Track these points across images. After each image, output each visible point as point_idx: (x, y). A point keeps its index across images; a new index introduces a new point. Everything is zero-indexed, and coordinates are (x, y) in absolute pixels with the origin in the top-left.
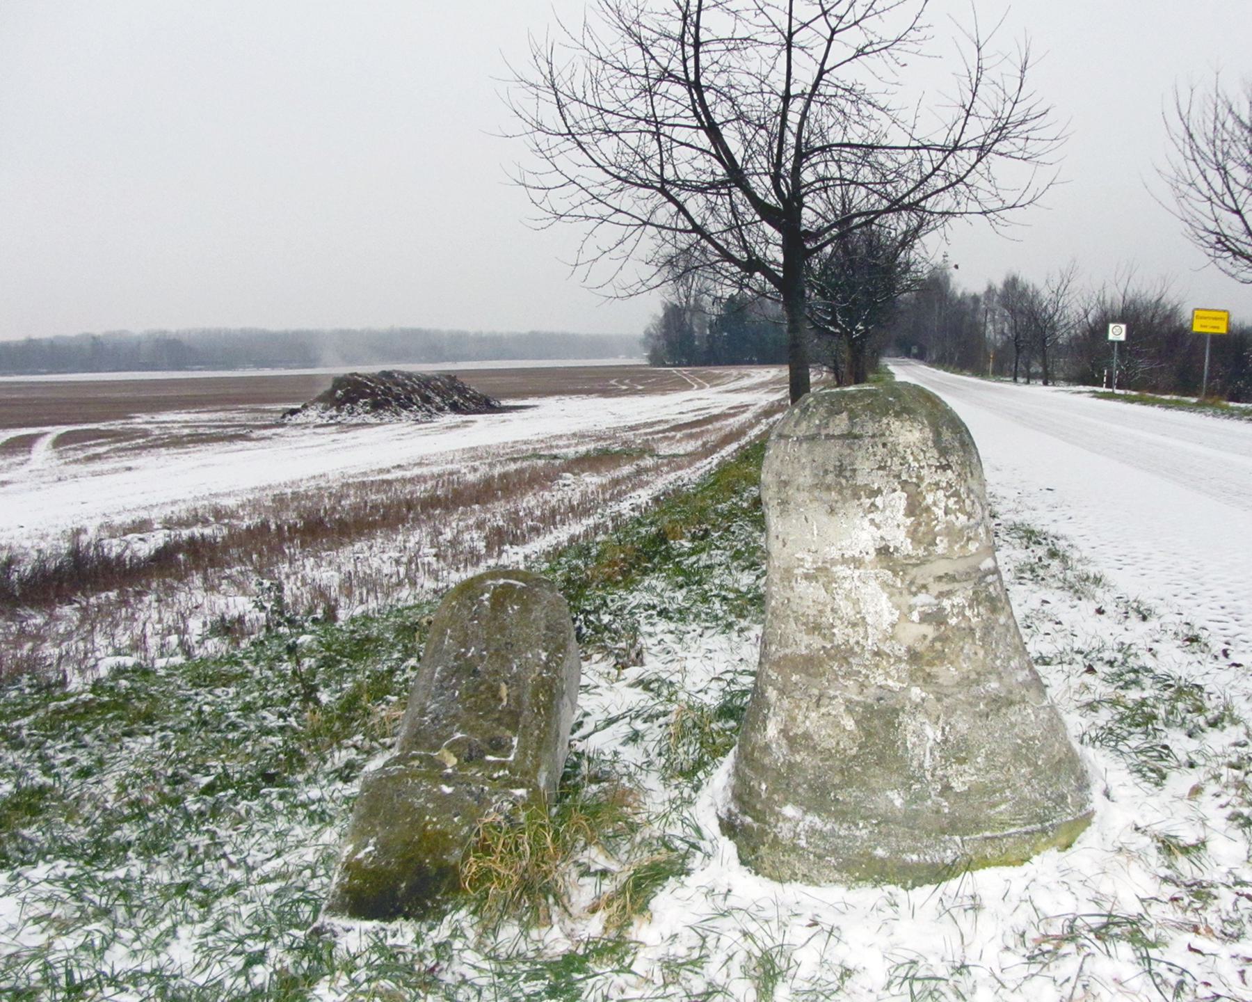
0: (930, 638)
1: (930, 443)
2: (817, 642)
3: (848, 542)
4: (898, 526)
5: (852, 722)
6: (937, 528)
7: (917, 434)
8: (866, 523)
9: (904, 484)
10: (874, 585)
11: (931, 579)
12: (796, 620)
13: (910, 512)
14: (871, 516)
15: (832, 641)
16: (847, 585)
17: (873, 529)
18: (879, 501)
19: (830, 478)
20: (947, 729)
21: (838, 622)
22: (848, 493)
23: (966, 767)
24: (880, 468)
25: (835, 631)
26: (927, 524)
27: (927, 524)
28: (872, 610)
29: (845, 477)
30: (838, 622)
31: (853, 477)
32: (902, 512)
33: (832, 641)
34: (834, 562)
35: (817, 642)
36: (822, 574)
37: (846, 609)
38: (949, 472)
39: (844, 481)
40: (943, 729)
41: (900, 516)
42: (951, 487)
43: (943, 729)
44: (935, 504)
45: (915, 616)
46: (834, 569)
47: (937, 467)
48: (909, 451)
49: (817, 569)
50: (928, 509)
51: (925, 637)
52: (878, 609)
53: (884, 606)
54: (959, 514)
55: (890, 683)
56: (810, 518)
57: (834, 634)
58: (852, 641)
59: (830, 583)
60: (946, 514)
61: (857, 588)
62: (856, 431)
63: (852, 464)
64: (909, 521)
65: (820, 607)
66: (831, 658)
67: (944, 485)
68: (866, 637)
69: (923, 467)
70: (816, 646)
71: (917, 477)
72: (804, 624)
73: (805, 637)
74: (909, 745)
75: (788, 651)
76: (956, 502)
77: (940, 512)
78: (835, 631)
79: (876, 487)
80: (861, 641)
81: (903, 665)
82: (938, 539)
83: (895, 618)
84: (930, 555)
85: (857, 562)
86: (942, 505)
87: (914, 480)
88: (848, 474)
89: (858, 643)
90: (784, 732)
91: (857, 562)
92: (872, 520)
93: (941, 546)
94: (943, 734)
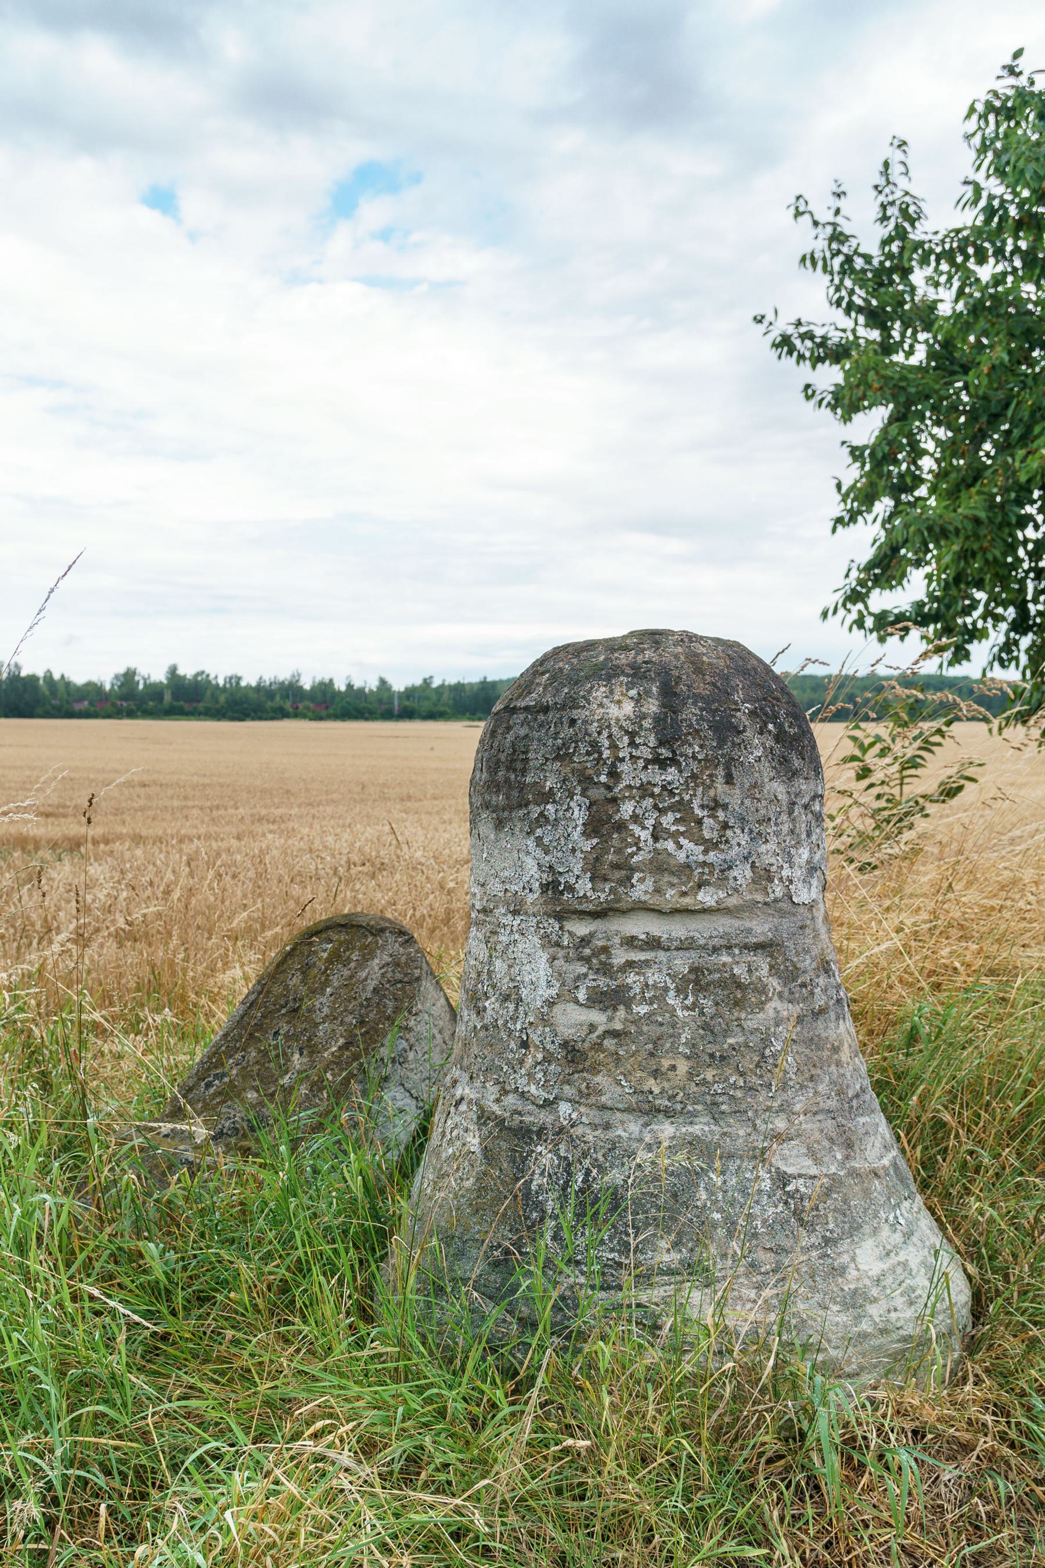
0: (600, 1030)
1: (647, 723)
4: (574, 850)
5: (476, 1141)
6: (635, 859)
7: (628, 708)
11: (617, 940)
13: (594, 827)
14: (539, 832)
17: (539, 853)
24: (558, 758)
26: (619, 851)
27: (619, 851)
29: (515, 770)
31: (524, 771)
40: (588, 1173)
41: (576, 835)
42: (672, 793)
43: (588, 1173)
44: (635, 818)
45: (582, 995)
48: (605, 734)
50: (621, 827)
51: (592, 1027)
54: (683, 841)
55: (533, 1089)
60: (656, 838)
63: (526, 752)
64: (587, 845)
68: (514, 1019)
69: (622, 760)
76: (677, 821)
77: (645, 835)
82: (637, 876)
83: (553, 992)
86: (650, 823)
87: (603, 778)
88: (519, 765)
92: (539, 840)
93: (641, 889)
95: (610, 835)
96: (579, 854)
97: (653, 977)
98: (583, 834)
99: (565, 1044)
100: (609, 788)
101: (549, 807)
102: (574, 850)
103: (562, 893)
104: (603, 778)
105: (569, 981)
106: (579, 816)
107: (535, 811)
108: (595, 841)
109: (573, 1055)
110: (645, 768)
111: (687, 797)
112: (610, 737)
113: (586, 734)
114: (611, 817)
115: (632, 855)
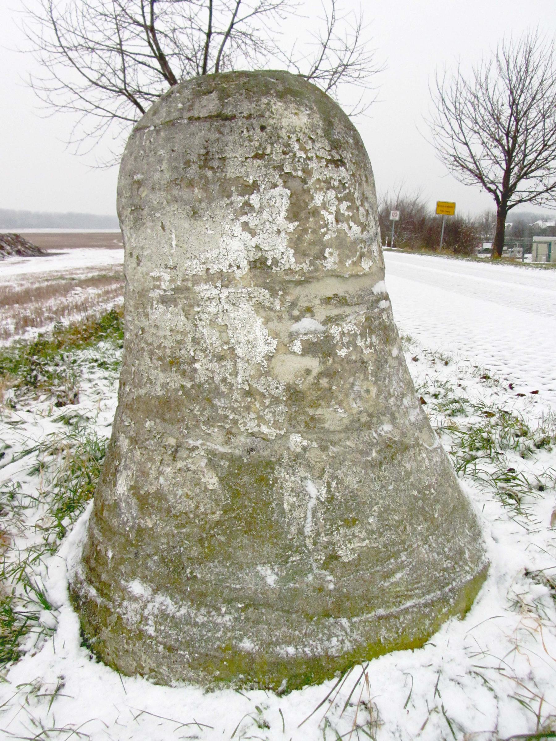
0: (314, 373)
1: (320, 132)
2: (175, 380)
3: (215, 253)
4: (279, 232)
5: (215, 480)
6: (327, 237)
8: (237, 229)
9: (287, 178)
10: (246, 307)
11: (317, 301)
12: (151, 354)
13: (294, 214)
14: (244, 219)
15: (192, 379)
16: (212, 308)
17: (246, 236)
18: (254, 199)
19: (193, 171)
20: (334, 484)
21: (200, 355)
22: (215, 188)
23: (356, 530)
24: (257, 156)
25: (197, 366)
26: (315, 232)
27: (315, 232)
28: (243, 339)
29: (212, 168)
30: (200, 355)
32: (283, 214)
33: (192, 379)
34: (196, 280)
35: (175, 380)
36: (181, 294)
37: (210, 336)
38: (342, 169)
39: (209, 174)
40: (329, 485)
41: (281, 220)
42: (344, 188)
43: (329, 485)
44: (324, 206)
45: (297, 347)
46: (197, 289)
47: (328, 161)
48: (294, 137)
49: (177, 290)
50: (315, 213)
51: (308, 371)
52: (251, 337)
53: (259, 334)
55: (264, 429)
56: (167, 225)
57: (195, 370)
58: (217, 379)
59: (192, 306)
60: (337, 221)
61: (225, 311)
62: (228, 111)
63: (222, 151)
64: (292, 226)
65: (179, 337)
66: (194, 399)
67: (336, 184)
68: (235, 374)
69: (310, 159)
70: (173, 385)
71: (304, 171)
72: (160, 359)
73: (161, 375)
74: (286, 507)
75: (142, 392)
76: (349, 208)
77: (331, 218)
78: (197, 366)
79: (251, 180)
80: (229, 379)
81: (281, 407)
82: (327, 251)
83: (272, 348)
84: (316, 270)
85: (225, 279)
86: (333, 209)
87: (300, 173)
88: (215, 164)
89: (224, 380)
90: (134, 489)
91: (225, 279)
92: (245, 225)
93: (331, 261)
94: (329, 492)
95: (307, 219)
96: (283, 234)
97: (348, 327)
98: (286, 218)
99: (288, 388)
100: (304, 181)
101: (252, 197)
102: (279, 232)
103: (270, 267)
104: (300, 173)
105: (285, 338)
106: (284, 204)
107: (239, 200)
108: (297, 223)
109: (294, 395)
110: (327, 166)
111: (352, 190)
112: (298, 140)
113: (279, 137)
114: (307, 204)
115: (324, 234)
